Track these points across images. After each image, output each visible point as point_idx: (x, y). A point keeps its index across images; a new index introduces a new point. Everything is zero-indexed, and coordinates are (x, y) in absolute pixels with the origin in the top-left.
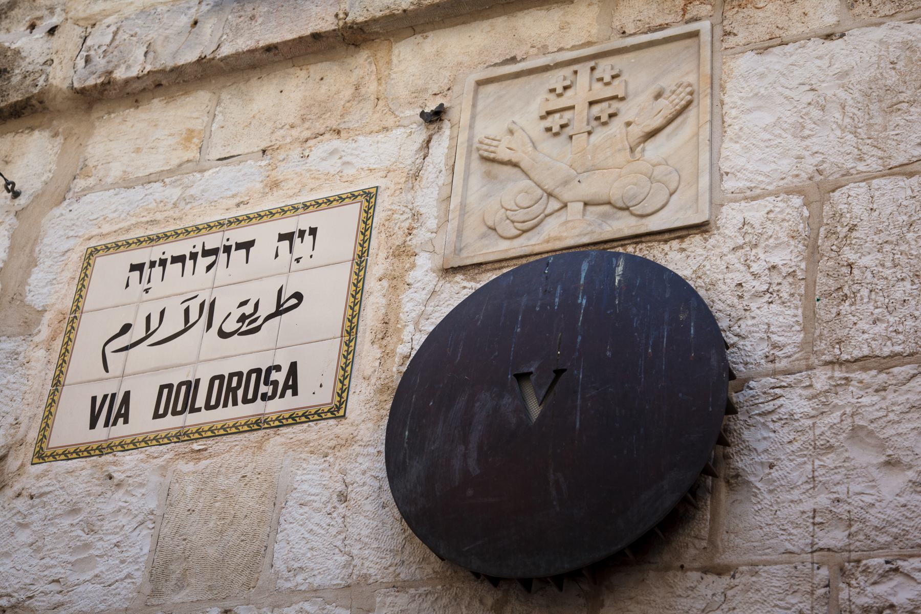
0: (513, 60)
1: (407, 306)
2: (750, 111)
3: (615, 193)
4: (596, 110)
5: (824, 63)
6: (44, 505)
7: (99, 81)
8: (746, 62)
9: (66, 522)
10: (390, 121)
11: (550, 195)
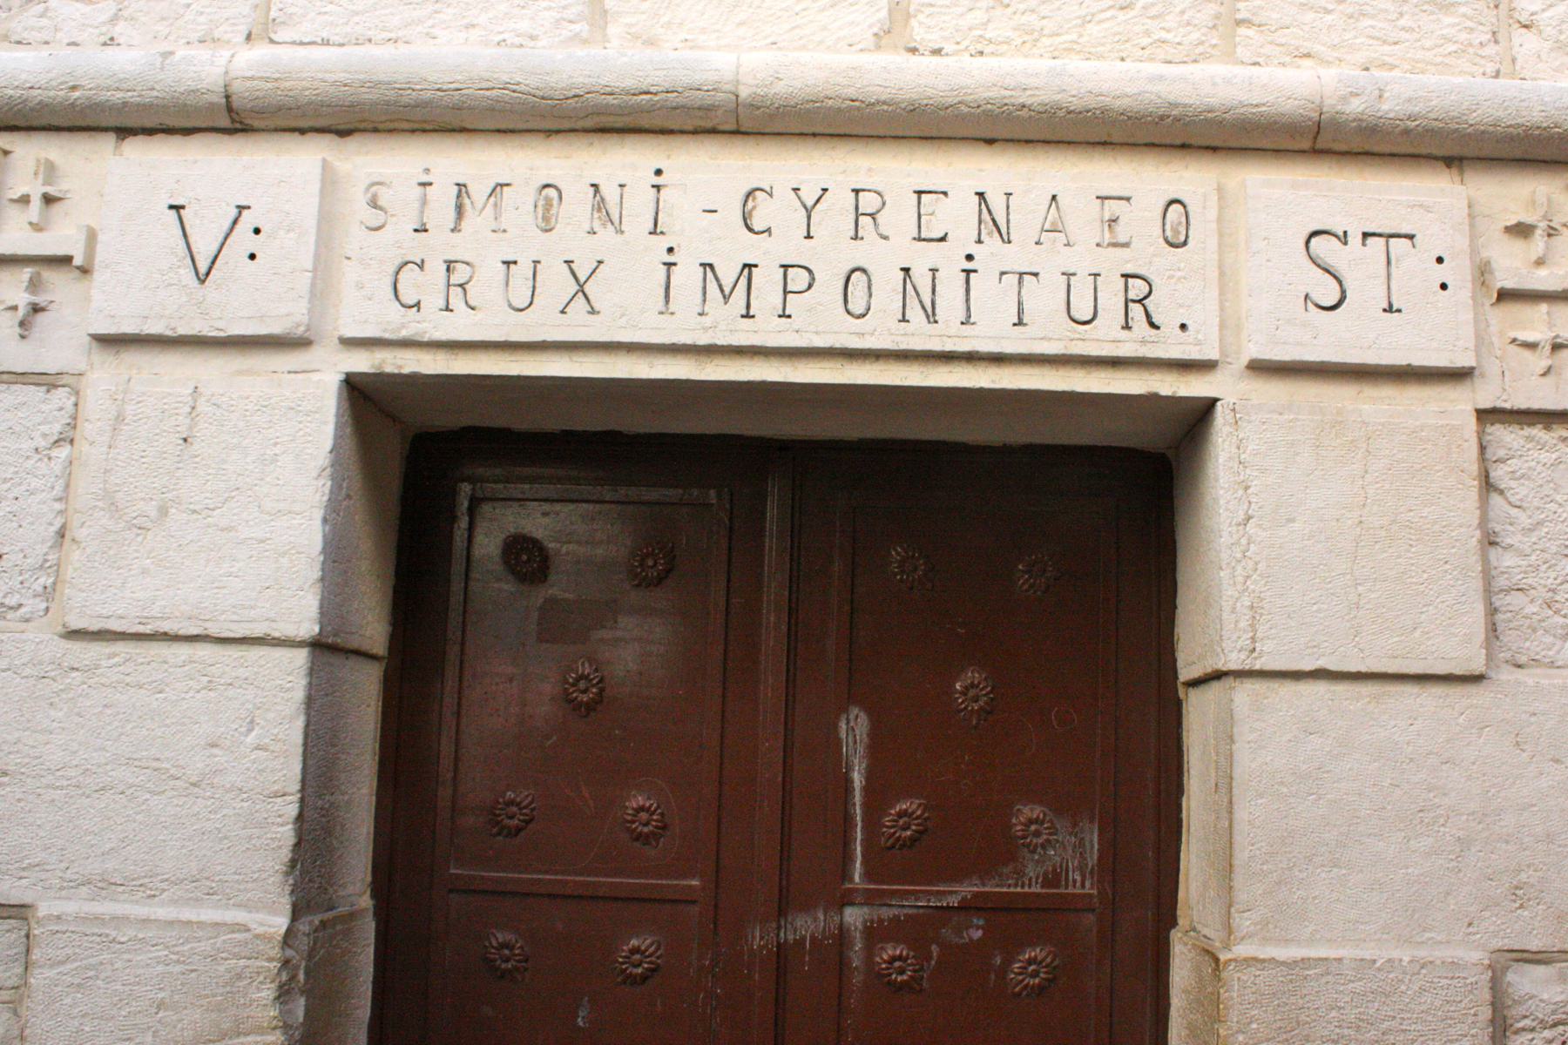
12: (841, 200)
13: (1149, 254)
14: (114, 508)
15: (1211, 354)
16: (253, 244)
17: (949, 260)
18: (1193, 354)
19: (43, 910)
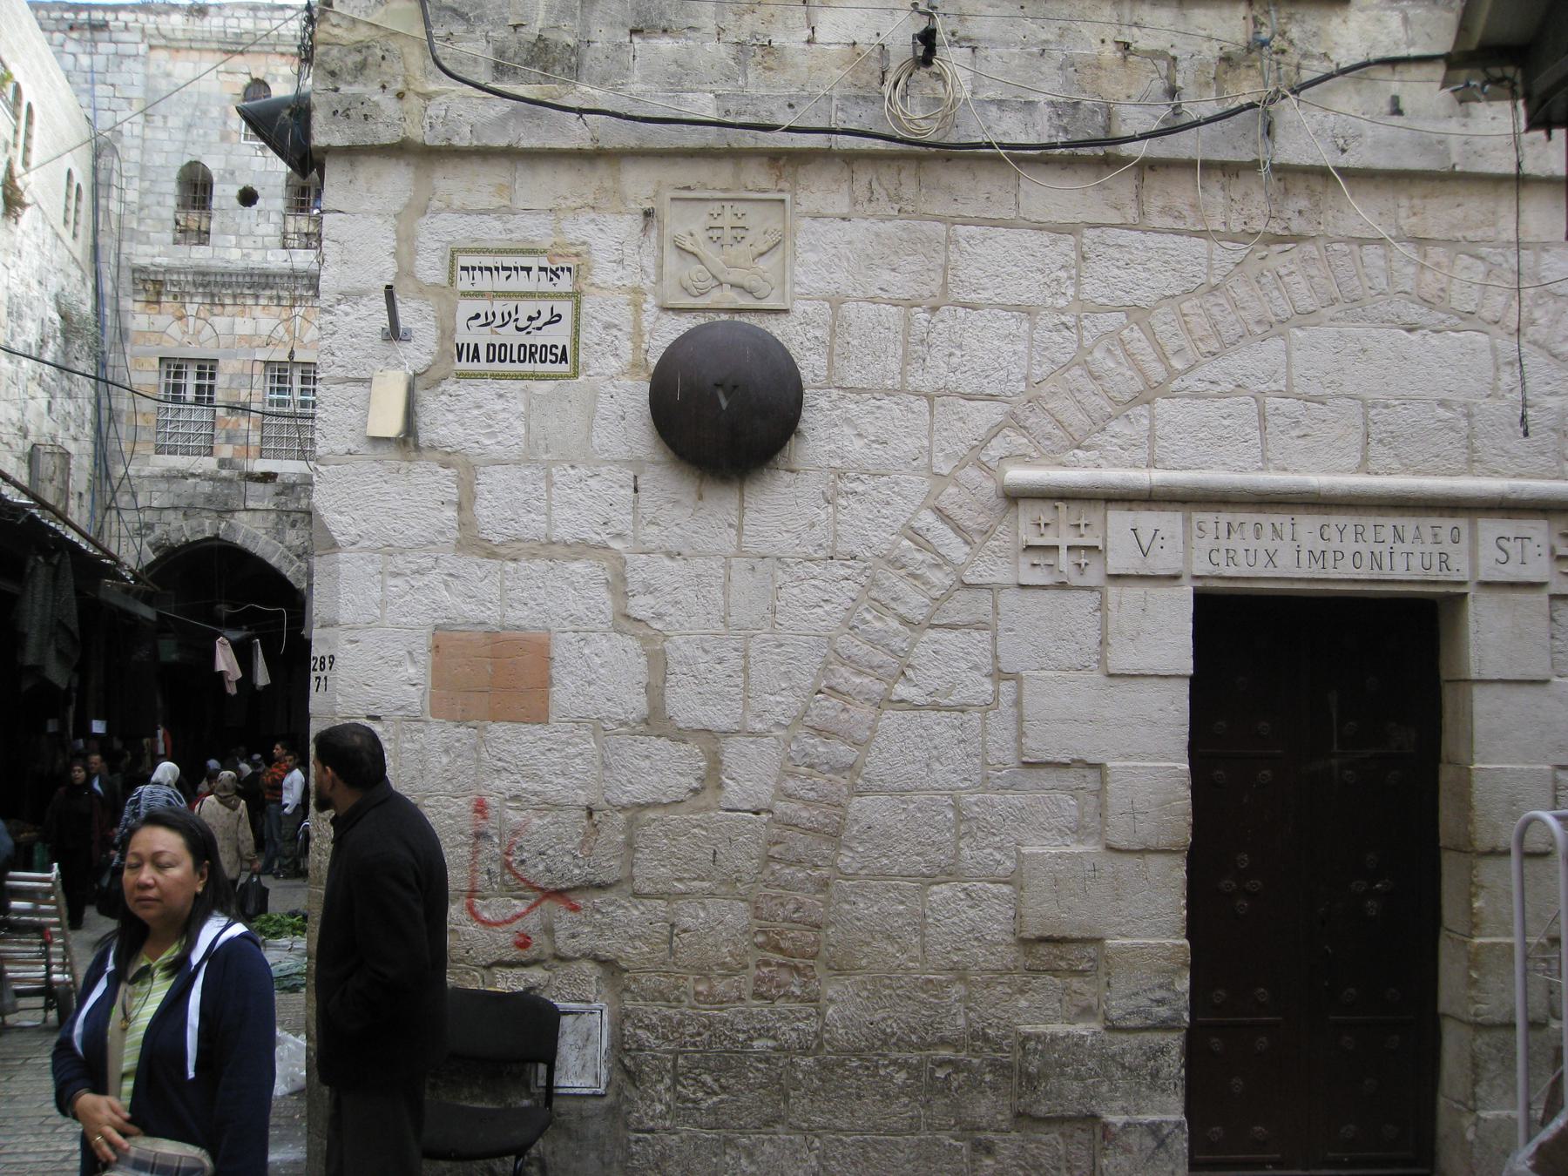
0: (688, 188)
1: (646, 324)
2: (806, 252)
3: (746, 284)
4: (734, 231)
5: (841, 234)
6: (460, 401)
7: (444, 143)
8: (805, 223)
9: (476, 412)
10: (622, 209)
11: (714, 277)
12: (1351, 529)
13: (1447, 546)
14: (1121, 633)
15: (1467, 579)
16: (1161, 543)
17: (1385, 548)
18: (1461, 579)
19: (1109, 764)
